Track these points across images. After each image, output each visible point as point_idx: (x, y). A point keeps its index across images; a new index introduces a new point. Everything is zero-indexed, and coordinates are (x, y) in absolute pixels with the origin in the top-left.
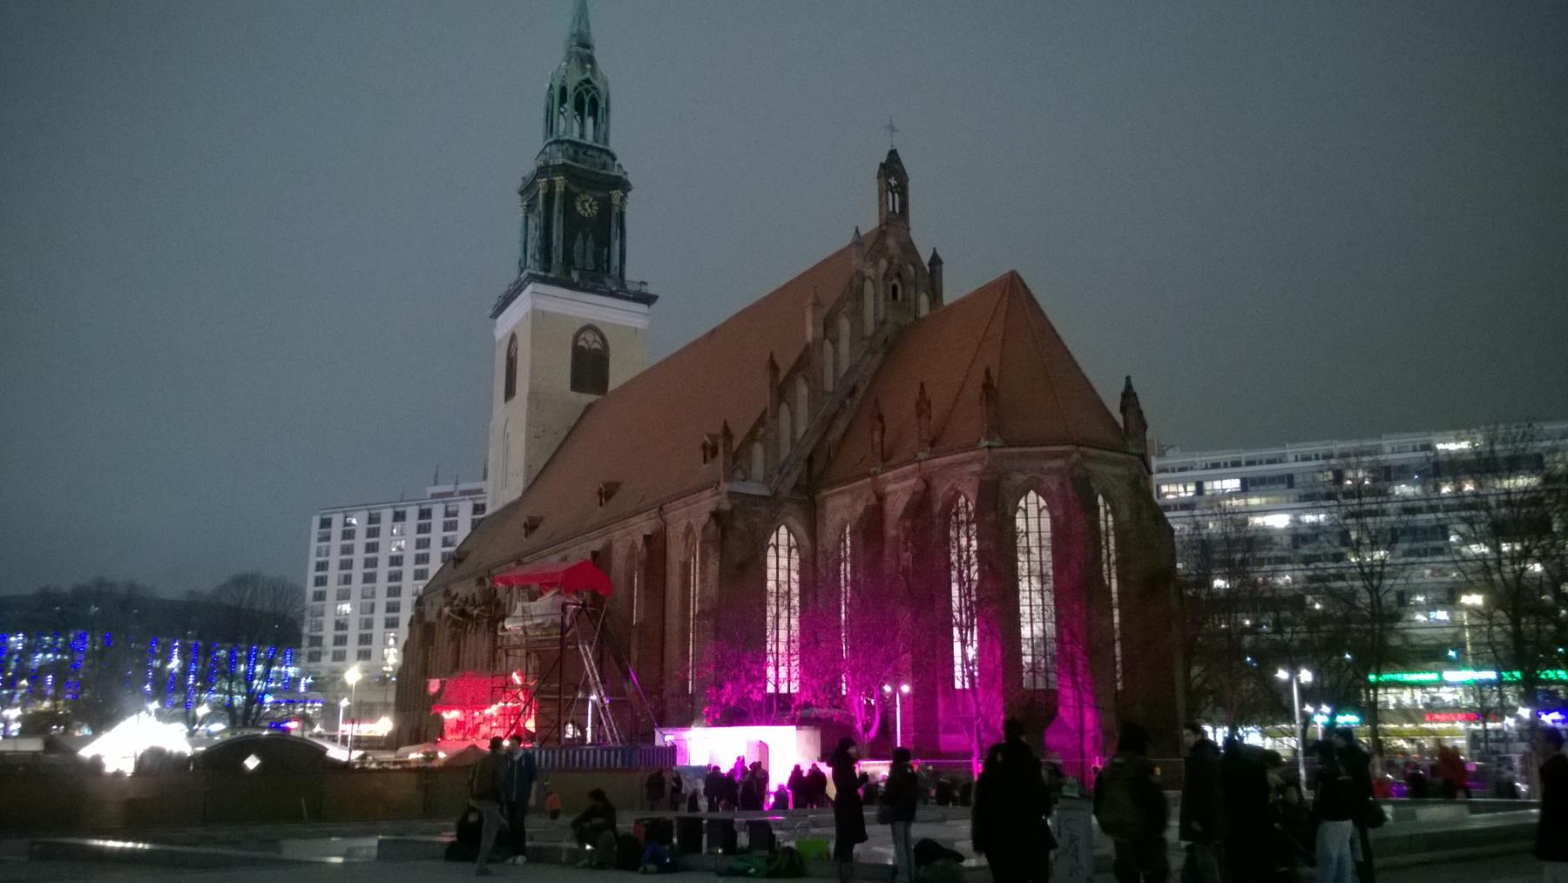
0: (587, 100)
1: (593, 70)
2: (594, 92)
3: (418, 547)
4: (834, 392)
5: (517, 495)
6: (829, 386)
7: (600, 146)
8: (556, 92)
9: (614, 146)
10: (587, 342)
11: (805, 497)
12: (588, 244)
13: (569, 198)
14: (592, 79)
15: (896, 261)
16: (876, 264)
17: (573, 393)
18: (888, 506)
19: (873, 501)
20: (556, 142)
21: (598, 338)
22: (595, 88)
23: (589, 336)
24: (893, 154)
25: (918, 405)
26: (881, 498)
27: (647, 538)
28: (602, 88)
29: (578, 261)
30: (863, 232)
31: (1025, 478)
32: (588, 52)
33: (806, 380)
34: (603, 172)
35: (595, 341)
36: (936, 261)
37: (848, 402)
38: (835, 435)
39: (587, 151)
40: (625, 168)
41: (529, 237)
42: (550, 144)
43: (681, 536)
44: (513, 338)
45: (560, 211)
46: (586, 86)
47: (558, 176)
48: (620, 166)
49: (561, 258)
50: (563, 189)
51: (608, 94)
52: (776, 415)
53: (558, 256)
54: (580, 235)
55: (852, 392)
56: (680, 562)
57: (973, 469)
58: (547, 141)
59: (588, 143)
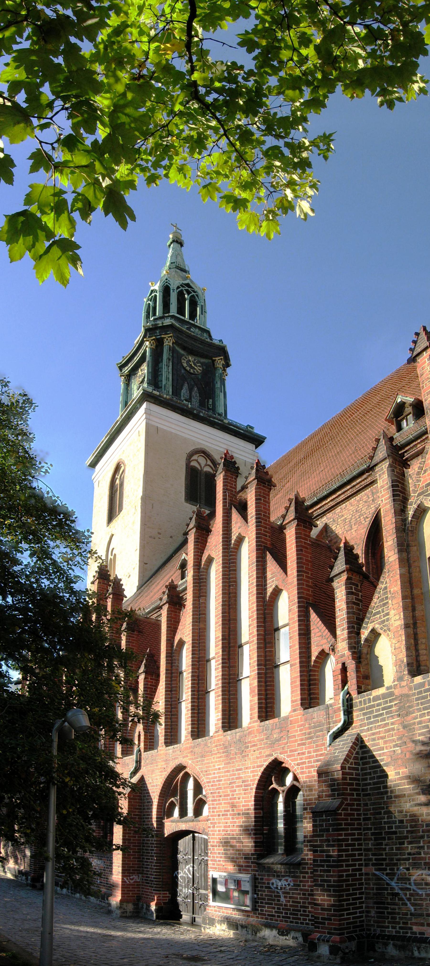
2: (193, 293)
14: (191, 284)
17: (188, 505)
21: (209, 463)
22: (194, 292)
23: (202, 461)
35: (206, 465)
39: (190, 328)
47: (166, 334)
54: (186, 386)
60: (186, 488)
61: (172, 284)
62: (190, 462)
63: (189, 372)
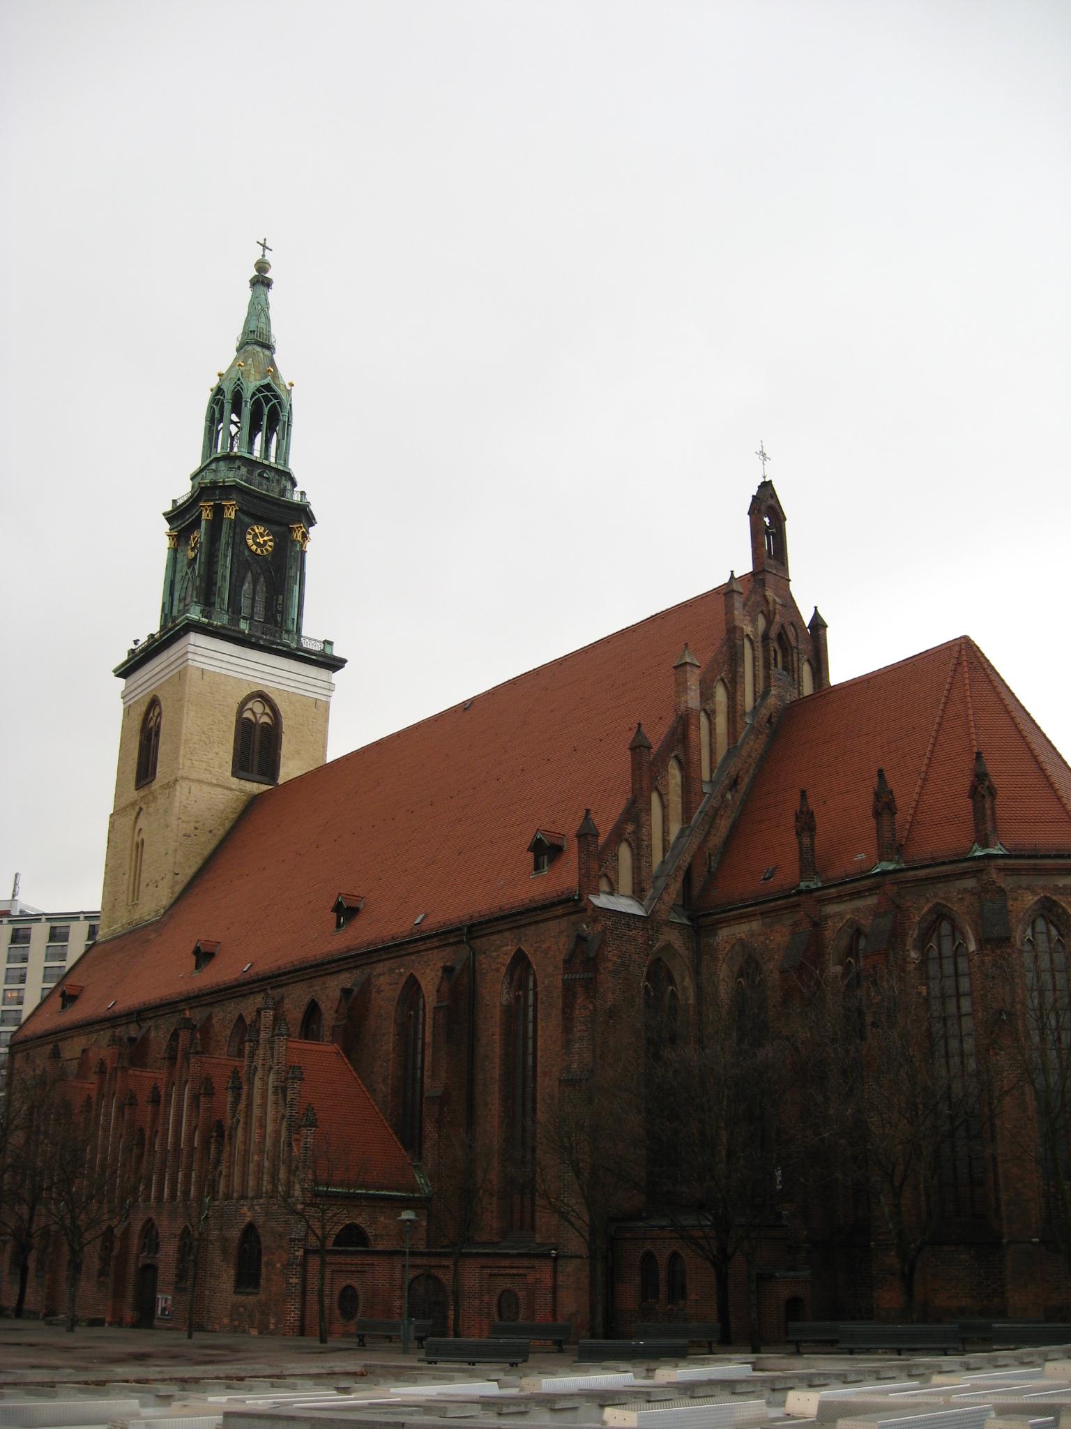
0: (266, 410)
1: (275, 375)
4: (711, 781)
6: (706, 776)
7: (280, 467)
8: (228, 396)
9: (295, 466)
10: (254, 713)
11: (685, 921)
12: (258, 588)
13: (239, 529)
14: (273, 385)
16: (754, 621)
17: (235, 780)
18: (829, 934)
21: (268, 710)
22: (277, 397)
23: (258, 707)
24: (766, 487)
25: (877, 796)
26: (817, 925)
27: (447, 970)
28: (283, 396)
29: (245, 612)
30: (737, 575)
31: (1036, 899)
32: (267, 352)
33: (679, 762)
34: (283, 498)
35: (264, 713)
36: (818, 624)
37: (729, 796)
38: (716, 840)
39: (264, 472)
40: (309, 498)
41: (178, 576)
42: (217, 460)
43: (503, 969)
44: (154, 703)
45: (227, 543)
46: (266, 393)
48: (303, 493)
49: (226, 602)
50: (233, 517)
51: (290, 405)
53: (223, 600)
55: (734, 784)
56: (501, 1005)
57: (966, 886)
58: (212, 458)
60: (235, 755)
61: (245, 391)
62: (242, 715)
63: (254, 554)
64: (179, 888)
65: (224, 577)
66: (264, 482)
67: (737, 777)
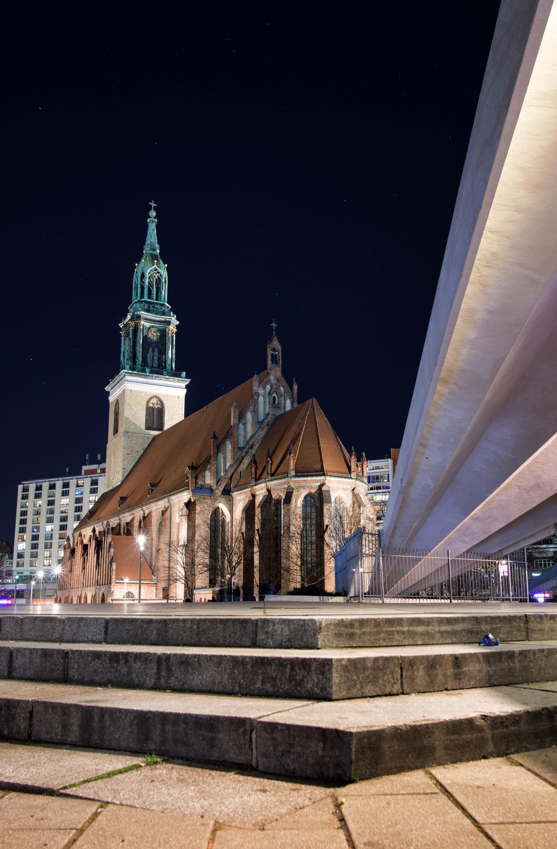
3: (76, 503)
5: (120, 483)
15: (274, 386)
16: (264, 388)
19: (251, 498)
20: (139, 302)
21: (159, 402)
26: (254, 496)
35: (157, 404)
42: (136, 303)
52: (216, 458)
54: (151, 349)
59: (155, 301)
64: (126, 474)
65: (139, 352)
66: (155, 310)
67: (253, 444)
